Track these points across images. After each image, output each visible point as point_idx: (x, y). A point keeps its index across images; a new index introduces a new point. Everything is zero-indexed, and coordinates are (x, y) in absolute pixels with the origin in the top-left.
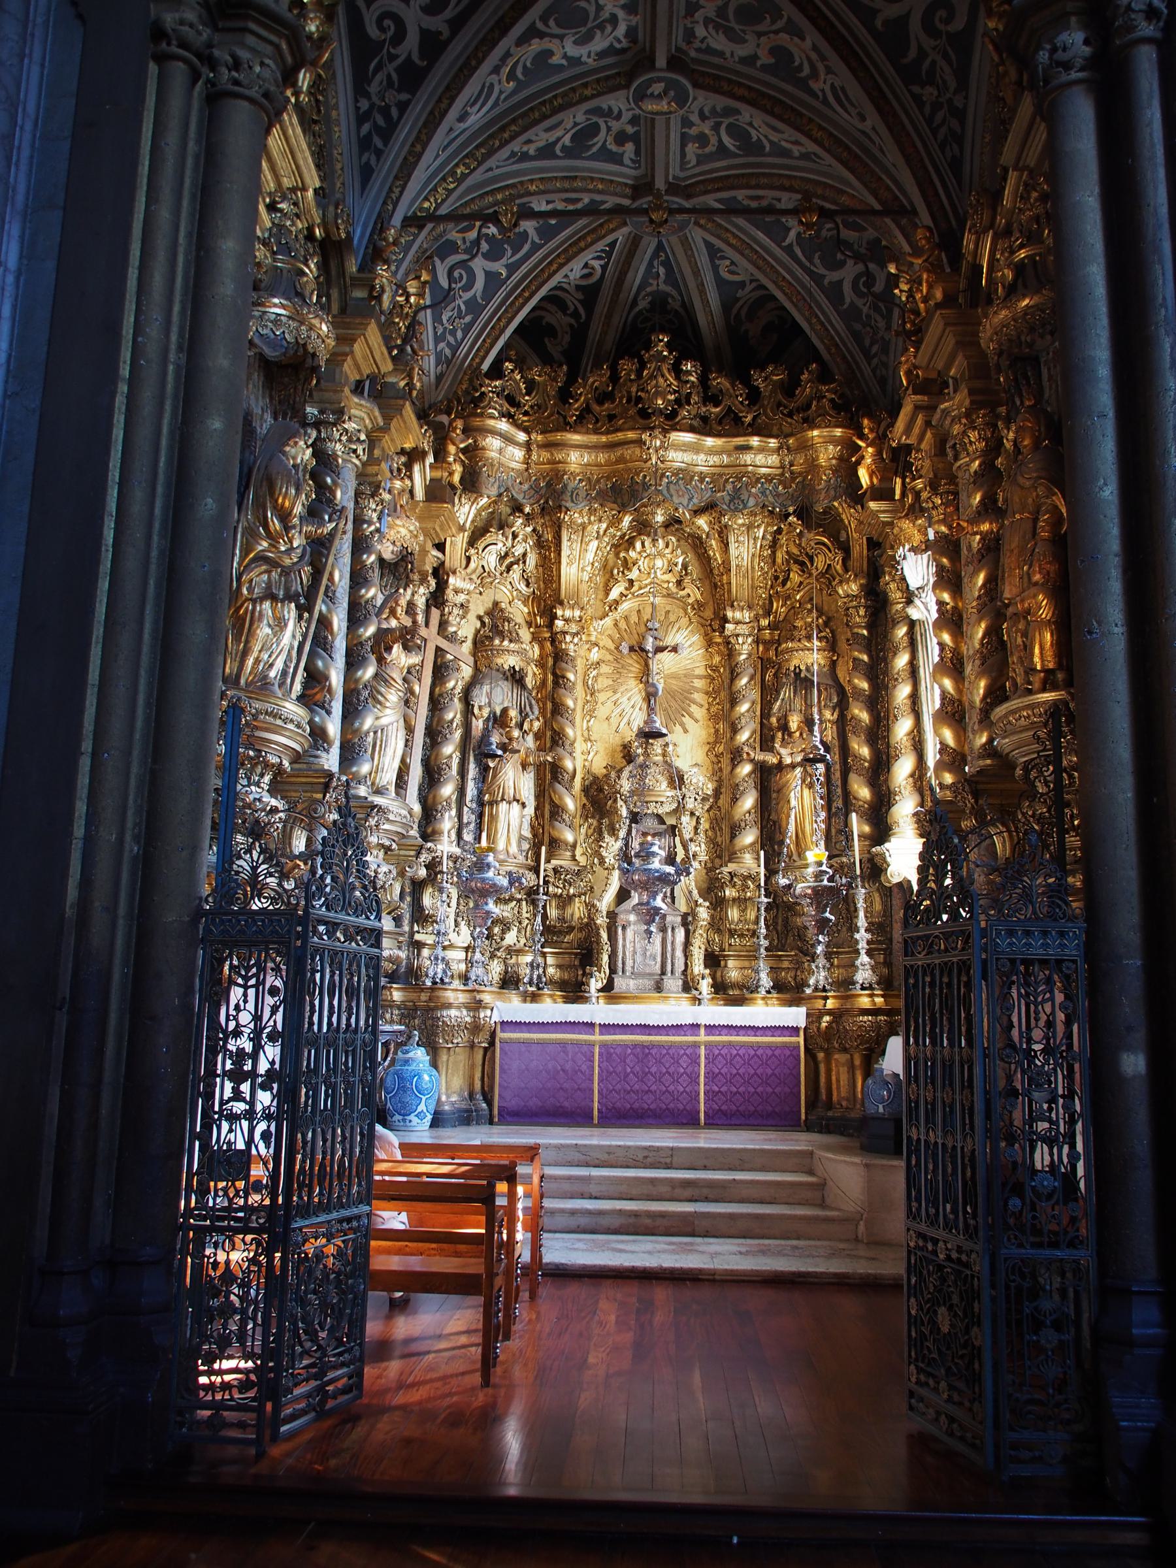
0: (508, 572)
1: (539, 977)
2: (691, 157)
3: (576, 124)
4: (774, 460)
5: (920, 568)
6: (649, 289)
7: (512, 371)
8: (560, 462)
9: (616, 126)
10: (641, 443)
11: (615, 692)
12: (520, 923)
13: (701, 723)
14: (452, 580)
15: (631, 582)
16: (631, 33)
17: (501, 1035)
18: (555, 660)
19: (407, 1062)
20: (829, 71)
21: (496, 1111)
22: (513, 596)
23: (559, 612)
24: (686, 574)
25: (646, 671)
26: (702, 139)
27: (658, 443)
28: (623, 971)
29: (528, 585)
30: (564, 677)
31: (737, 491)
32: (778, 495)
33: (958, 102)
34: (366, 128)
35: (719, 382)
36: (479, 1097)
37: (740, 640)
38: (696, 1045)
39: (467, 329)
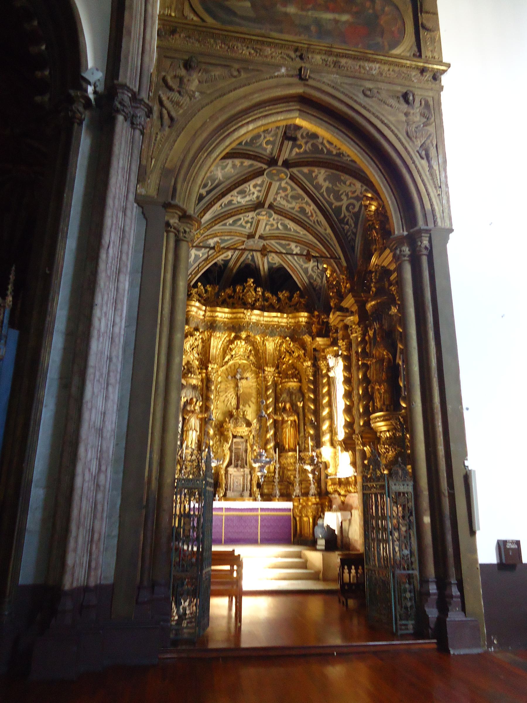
4: (285, 320)
9: (246, 219)
10: (244, 313)
11: (226, 392)
15: (232, 356)
16: (258, 197)
18: (207, 381)
20: (316, 216)
25: (237, 386)
26: (272, 225)
33: (354, 230)
35: (267, 295)
38: (257, 516)
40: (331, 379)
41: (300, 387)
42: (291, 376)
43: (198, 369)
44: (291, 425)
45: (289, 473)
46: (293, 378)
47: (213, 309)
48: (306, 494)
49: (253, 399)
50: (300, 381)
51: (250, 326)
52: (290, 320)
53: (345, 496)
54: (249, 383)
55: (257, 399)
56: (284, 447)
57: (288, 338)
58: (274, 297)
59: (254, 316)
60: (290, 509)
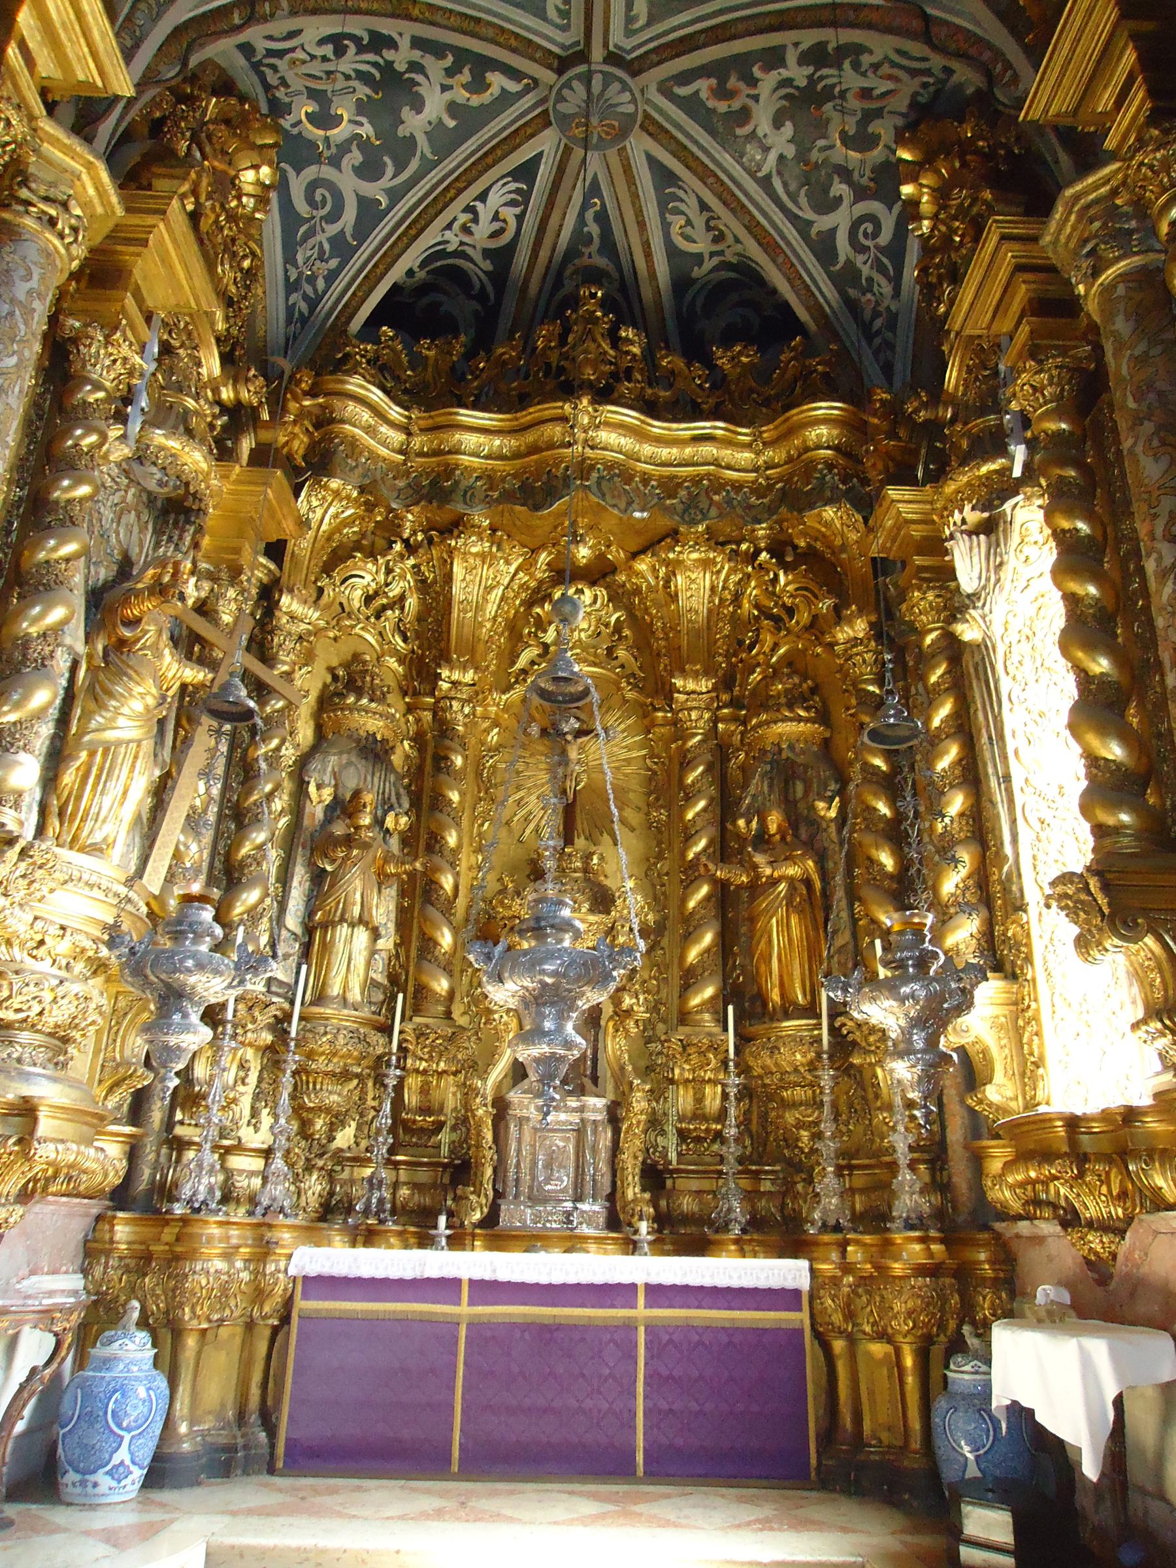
0: (378, 617)
1: (381, 1201)
4: (745, 457)
5: (976, 559)
7: (391, 339)
8: (450, 452)
12: (362, 1115)
13: (637, 832)
14: (285, 600)
15: (546, 646)
17: (301, 1305)
19: (107, 1363)
21: (281, 1449)
22: (383, 646)
23: (445, 673)
24: (620, 638)
25: (564, 760)
27: (586, 421)
28: (516, 1196)
29: (405, 640)
30: (447, 758)
32: (750, 507)
36: (254, 1418)
38: (629, 1327)
39: (331, 277)
40: (968, 661)
41: (826, 743)
42: (783, 700)
43: (405, 694)
44: (789, 898)
45: (790, 1117)
46: (790, 706)
48: (876, 1219)
50: (824, 717)
51: (595, 475)
52: (769, 453)
53: (1117, 1229)
54: (612, 753)
55: (648, 814)
56: (761, 998)
57: (764, 556)
58: (698, 369)
59: (613, 433)
60: (797, 1293)
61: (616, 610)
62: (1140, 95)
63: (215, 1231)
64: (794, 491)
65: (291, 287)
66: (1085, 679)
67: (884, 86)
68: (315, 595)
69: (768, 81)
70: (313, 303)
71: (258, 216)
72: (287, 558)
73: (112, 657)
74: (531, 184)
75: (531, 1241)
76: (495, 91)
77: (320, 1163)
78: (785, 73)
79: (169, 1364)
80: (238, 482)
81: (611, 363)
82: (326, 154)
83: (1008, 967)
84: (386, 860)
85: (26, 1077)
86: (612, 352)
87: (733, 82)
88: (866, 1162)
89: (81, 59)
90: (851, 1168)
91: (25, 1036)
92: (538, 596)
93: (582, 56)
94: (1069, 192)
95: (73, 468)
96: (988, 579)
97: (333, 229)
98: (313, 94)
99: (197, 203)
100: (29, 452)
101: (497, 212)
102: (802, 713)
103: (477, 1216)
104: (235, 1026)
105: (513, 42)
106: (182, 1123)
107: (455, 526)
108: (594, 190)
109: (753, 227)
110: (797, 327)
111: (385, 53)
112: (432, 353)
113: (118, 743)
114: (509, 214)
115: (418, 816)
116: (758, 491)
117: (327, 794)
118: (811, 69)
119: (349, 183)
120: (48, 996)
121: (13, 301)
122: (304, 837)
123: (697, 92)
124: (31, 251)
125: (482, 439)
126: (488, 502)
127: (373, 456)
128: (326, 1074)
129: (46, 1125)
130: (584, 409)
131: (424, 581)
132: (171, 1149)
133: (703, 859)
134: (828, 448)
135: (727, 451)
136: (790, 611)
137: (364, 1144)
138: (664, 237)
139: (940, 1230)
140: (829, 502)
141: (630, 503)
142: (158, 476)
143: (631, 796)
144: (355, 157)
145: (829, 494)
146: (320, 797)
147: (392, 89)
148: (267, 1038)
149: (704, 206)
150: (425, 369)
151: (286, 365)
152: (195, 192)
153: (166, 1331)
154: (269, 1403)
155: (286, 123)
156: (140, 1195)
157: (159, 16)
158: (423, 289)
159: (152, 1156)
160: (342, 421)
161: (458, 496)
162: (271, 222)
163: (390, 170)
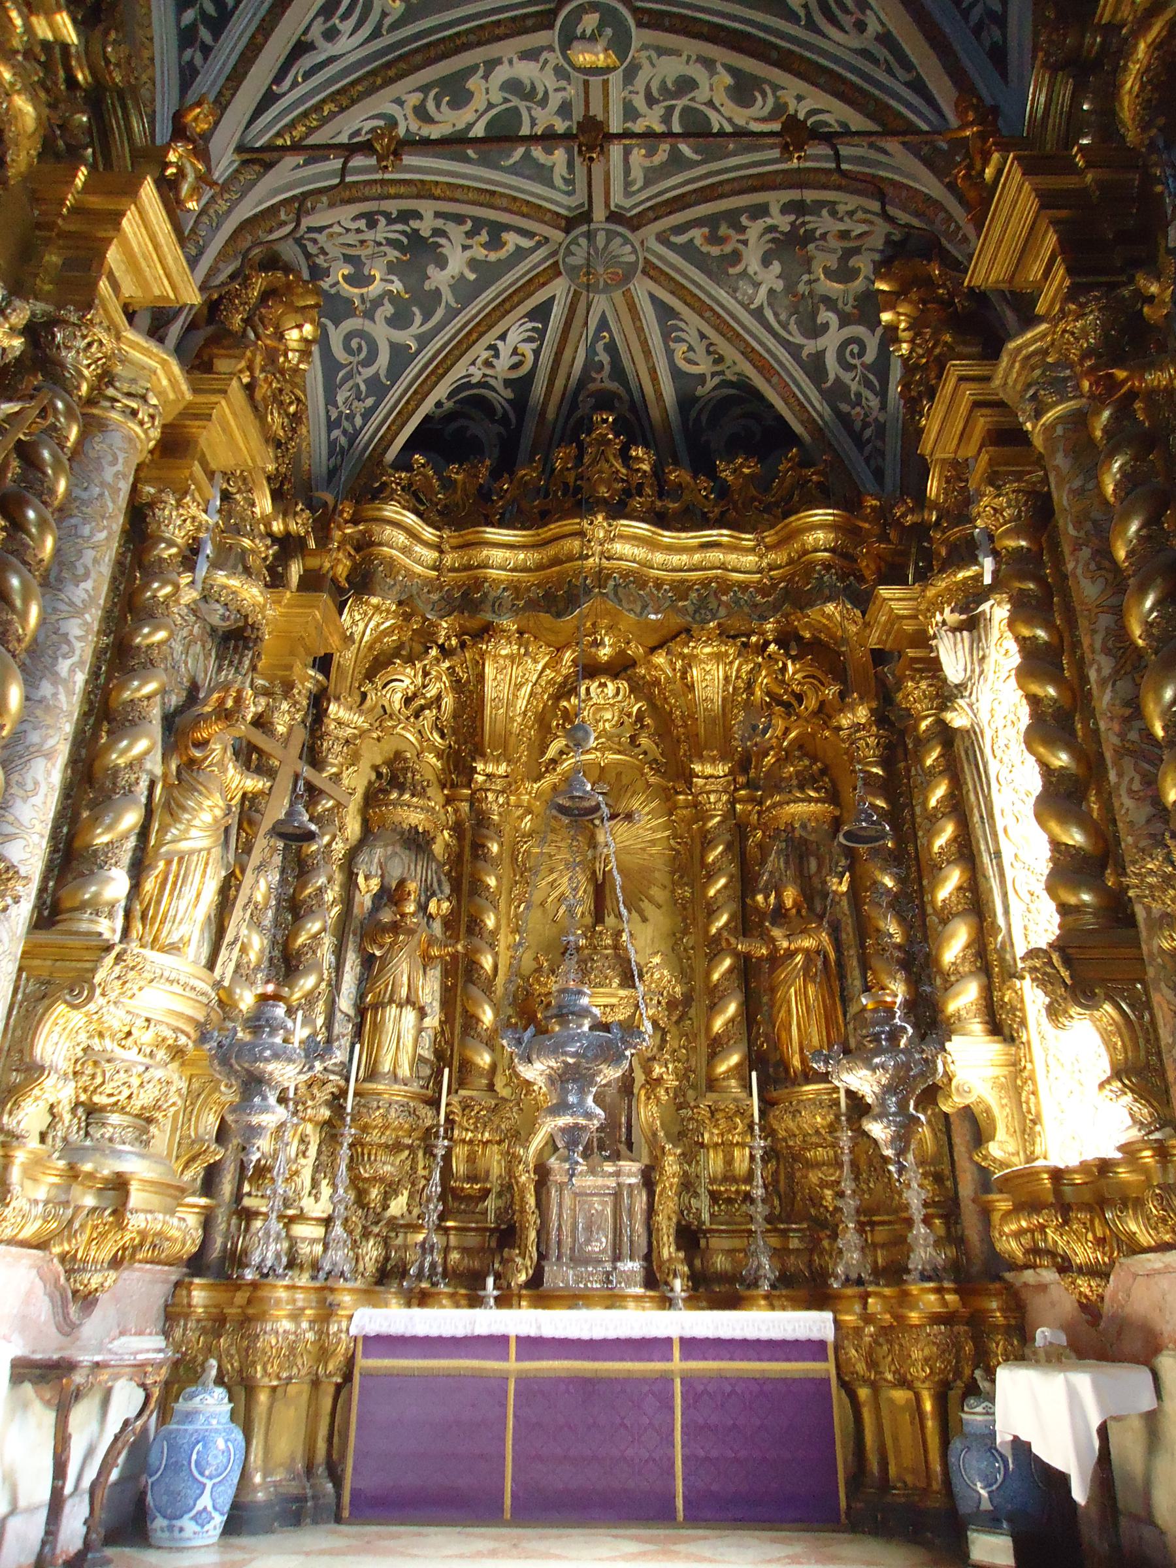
0: (417, 717)
1: (433, 1265)
2: (637, 174)
3: (490, 106)
4: (750, 560)
5: (960, 653)
6: (592, 387)
7: (423, 466)
8: (479, 567)
10: (581, 534)
12: (413, 1184)
13: (664, 909)
14: (333, 708)
17: (362, 1363)
19: (189, 1416)
22: (423, 744)
23: (480, 766)
24: (642, 727)
25: (593, 844)
28: (559, 1258)
29: (443, 736)
30: (483, 846)
31: (703, 599)
32: (756, 605)
34: (189, 16)
36: (321, 1470)
37: (712, 798)
38: (666, 1380)
39: (367, 415)
40: (959, 746)
42: (794, 782)
43: (443, 787)
44: (806, 968)
45: (814, 1177)
46: (802, 788)
47: (469, 535)
48: (894, 1273)
49: (655, 892)
50: (834, 797)
51: (611, 583)
52: (772, 556)
54: (637, 836)
55: (673, 891)
56: (784, 1064)
57: (772, 647)
58: (703, 482)
59: (628, 545)
60: (822, 1344)
61: (637, 700)
62: (1061, 271)
63: (282, 1294)
64: (794, 590)
65: (331, 425)
66: (1047, 771)
67: (860, 229)
68: (358, 700)
69: (754, 229)
70: (352, 438)
71: (302, 366)
72: (333, 670)
73: (185, 775)
74: (545, 321)
75: (573, 1299)
76: (510, 248)
77: (376, 1230)
78: (769, 221)
79: (244, 1419)
80: (288, 606)
81: (623, 481)
82: (362, 308)
83: (1006, 1031)
84: (430, 944)
85: (118, 1154)
86: (624, 471)
87: (723, 230)
88: (882, 1215)
89: (157, 279)
90: (873, 1224)
91: (115, 1118)
92: (566, 689)
93: (586, 217)
94: (1012, 345)
95: (152, 616)
96: (973, 671)
97: (368, 372)
98: (348, 259)
99: (252, 376)
100: (115, 604)
101: (516, 348)
102: (812, 794)
103: (522, 1278)
104: (296, 1104)
105: (525, 209)
106: (249, 1194)
107: (486, 631)
108: (603, 324)
109: (749, 353)
110: (794, 439)
111: (411, 222)
112: (459, 477)
113: (191, 853)
114: (527, 349)
115: (459, 901)
116: (763, 591)
117: (375, 884)
118: (792, 218)
119: (382, 332)
120: (135, 1081)
121: (103, 484)
122: (355, 924)
123: (691, 240)
124: (116, 439)
125: (508, 554)
126: (515, 611)
127: (410, 574)
128: (380, 1146)
129: (136, 1197)
130: (598, 527)
131: (458, 681)
132: (240, 1219)
133: (725, 934)
134: (825, 550)
135: (734, 556)
136: (800, 698)
137: (416, 1212)
138: (668, 361)
139: (955, 1281)
140: (829, 599)
141: (644, 607)
142: (221, 611)
143: (657, 874)
144: (388, 309)
145: (827, 592)
146: (367, 887)
147: (419, 251)
148: (325, 1113)
149: (703, 336)
150: (455, 492)
151: (329, 498)
152: (250, 368)
153: (240, 1387)
154: (335, 1457)
155: (325, 285)
156: (213, 1263)
157: (218, 227)
158: (451, 416)
159: (223, 1226)
160: (381, 544)
161: (487, 606)
162: (314, 371)
163: (418, 319)
